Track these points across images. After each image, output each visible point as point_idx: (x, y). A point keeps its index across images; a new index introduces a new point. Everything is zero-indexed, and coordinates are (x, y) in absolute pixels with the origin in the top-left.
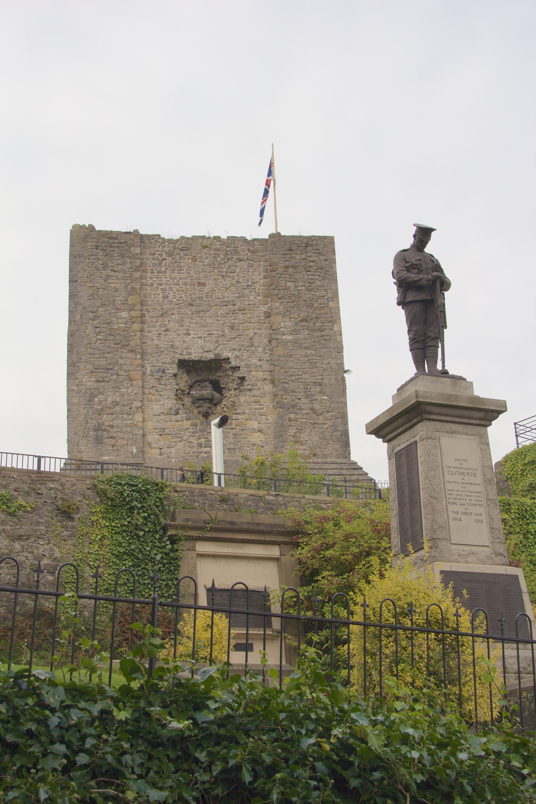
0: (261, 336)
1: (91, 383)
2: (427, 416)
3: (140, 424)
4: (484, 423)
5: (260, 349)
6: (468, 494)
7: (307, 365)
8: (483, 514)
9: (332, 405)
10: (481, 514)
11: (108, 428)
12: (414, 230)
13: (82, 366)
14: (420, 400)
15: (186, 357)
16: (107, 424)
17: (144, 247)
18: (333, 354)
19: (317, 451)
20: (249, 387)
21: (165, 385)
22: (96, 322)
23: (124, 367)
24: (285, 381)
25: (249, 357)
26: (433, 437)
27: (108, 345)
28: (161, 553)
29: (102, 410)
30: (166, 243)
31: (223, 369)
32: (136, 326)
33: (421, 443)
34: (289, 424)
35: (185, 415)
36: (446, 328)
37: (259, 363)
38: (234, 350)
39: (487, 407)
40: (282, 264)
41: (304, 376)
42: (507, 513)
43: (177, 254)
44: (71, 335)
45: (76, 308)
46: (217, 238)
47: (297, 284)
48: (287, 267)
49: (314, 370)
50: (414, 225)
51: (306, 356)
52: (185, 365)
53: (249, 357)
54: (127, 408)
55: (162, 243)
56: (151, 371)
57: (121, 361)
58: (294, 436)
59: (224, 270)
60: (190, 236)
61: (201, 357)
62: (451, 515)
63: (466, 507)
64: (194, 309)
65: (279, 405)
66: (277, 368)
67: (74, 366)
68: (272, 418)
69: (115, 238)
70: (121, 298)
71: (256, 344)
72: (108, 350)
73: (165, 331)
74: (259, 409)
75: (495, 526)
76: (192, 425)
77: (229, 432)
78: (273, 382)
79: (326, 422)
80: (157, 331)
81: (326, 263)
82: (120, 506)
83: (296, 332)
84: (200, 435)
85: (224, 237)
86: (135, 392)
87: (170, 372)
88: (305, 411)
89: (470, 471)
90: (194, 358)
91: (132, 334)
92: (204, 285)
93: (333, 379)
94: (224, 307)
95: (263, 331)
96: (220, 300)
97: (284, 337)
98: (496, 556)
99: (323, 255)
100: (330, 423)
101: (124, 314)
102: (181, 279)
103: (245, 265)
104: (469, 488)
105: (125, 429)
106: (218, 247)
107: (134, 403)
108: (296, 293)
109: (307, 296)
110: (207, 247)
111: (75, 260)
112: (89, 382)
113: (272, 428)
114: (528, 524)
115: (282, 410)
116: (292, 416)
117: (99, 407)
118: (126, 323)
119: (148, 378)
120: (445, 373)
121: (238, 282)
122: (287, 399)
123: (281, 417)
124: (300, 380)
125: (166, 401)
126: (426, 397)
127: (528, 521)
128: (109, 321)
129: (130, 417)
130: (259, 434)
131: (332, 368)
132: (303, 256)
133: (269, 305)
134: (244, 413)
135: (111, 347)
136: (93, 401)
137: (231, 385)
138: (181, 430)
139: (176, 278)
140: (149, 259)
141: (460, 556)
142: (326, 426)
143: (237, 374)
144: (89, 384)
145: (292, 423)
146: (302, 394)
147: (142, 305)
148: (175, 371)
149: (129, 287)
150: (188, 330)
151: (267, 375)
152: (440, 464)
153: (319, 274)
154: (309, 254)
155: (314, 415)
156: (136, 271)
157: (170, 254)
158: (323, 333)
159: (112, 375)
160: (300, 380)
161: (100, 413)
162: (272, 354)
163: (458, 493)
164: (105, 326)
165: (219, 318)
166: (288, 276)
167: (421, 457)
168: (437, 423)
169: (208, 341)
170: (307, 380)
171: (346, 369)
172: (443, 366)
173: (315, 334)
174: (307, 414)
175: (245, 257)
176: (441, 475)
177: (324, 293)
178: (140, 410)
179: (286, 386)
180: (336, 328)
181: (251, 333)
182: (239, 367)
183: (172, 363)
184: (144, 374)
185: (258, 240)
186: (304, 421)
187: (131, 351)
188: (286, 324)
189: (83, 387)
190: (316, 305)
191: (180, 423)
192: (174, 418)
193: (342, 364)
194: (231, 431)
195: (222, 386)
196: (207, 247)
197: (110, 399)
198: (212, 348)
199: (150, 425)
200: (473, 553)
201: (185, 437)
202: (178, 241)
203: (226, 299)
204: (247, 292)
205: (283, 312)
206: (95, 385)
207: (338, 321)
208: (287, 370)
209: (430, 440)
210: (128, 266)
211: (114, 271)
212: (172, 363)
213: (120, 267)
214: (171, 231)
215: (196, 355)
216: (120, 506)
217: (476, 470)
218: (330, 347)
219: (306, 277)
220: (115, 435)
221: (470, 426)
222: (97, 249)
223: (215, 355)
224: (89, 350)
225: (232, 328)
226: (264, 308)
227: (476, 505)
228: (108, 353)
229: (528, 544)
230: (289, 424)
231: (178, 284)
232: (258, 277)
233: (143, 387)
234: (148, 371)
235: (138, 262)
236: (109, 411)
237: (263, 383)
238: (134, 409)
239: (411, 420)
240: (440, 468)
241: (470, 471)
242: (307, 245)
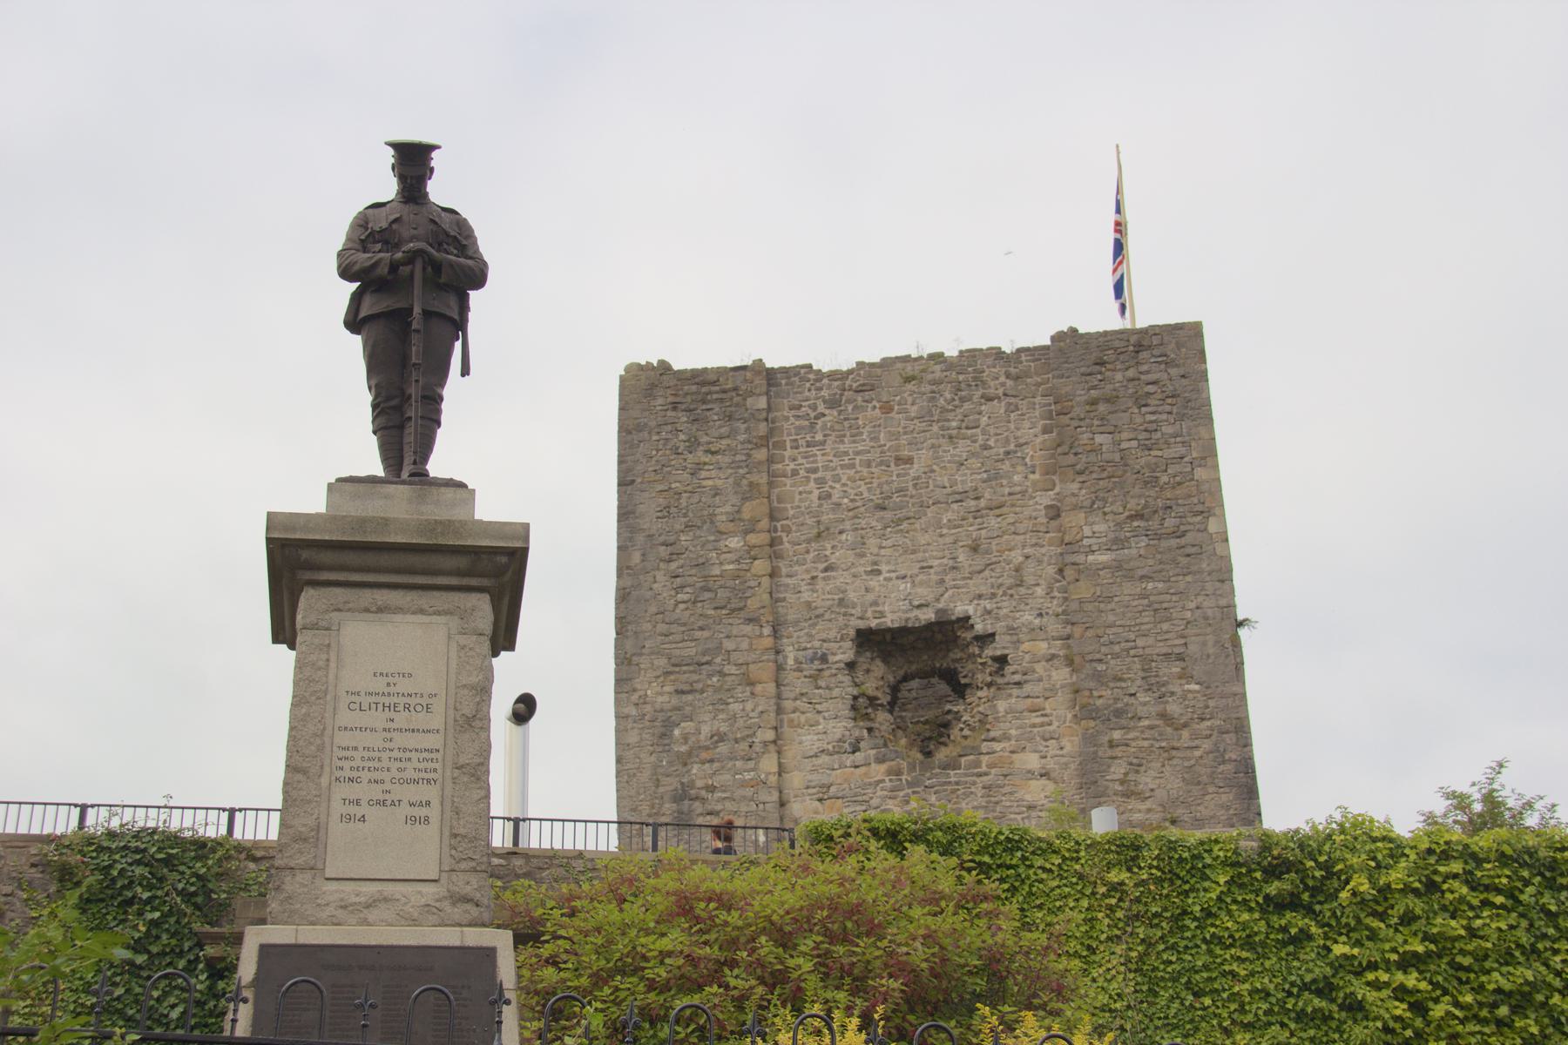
0: (1040, 562)
1: (666, 698)
2: (308, 575)
3: (773, 779)
5: (1039, 591)
6: (401, 755)
7: (1147, 617)
8: (436, 803)
9: (1211, 703)
10: (428, 803)
11: (703, 793)
12: (389, 156)
13: (644, 662)
15: (873, 624)
16: (699, 783)
17: (777, 395)
18: (1209, 586)
19: (1180, 811)
20: (1017, 678)
21: (828, 688)
22: (673, 566)
23: (734, 656)
24: (1098, 656)
25: (1015, 610)
27: (699, 611)
28: (184, 1001)
29: (690, 754)
30: (825, 381)
31: (960, 642)
32: (761, 566)
34: (1110, 753)
35: (873, 752)
37: (1037, 621)
38: (980, 597)
39: (469, 543)
40: (1081, 396)
41: (1140, 642)
42: (1129, 870)
43: (849, 401)
44: (623, 597)
45: (631, 539)
46: (937, 357)
47: (1117, 437)
48: (1094, 402)
49: (1165, 626)
51: (1143, 596)
52: (871, 641)
53: (1015, 610)
54: (744, 746)
55: (817, 380)
56: (796, 660)
57: (729, 645)
58: (1122, 782)
59: (954, 424)
60: (877, 360)
61: (907, 620)
62: (337, 808)
63: (387, 786)
64: (888, 515)
65: (1086, 713)
66: (1078, 631)
67: (630, 664)
68: (1070, 745)
69: (714, 383)
70: (728, 508)
71: (1030, 580)
72: (700, 623)
73: (826, 570)
74: (1042, 725)
75: (462, 831)
76: (889, 773)
77: (974, 783)
78: (1070, 662)
79: (1197, 742)
80: (807, 571)
82: (102, 900)
83: (1119, 543)
84: (907, 795)
85: (951, 352)
86: (760, 708)
87: (838, 658)
88: (1146, 723)
89: (412, 701)
90: (890, 624)
91: (752, 583)
92: (910, 461)
93: (1210, 643)
94: (955, 506)
95: (1043, 550)
96: (949, 490)
97: (1091, 558)
98: (454, 904)
99: (1177, 366)
100: (1207, 745)
101: (734, 543)
102: (858, 453)
103: (1000, 408)
104: (400, 740)
105: (739, 793)
106: (938, 375)
107: (759, 733)
108: (1117, 457)
109: (1143, 461)
110: (913, 378)
111: (629, 438)
112: (659, 695)
113: (1072, 766)
114: (1186, 893)
115: (1092, 723)
116: (1117, 735)
117: (684, 748)
118: (738, 561)
119: (790, 677)
121: (986, 447)
122: (1104, 697)
123: (1089, 739)
124: (1132, 652)
125: (832, 723)
127: (1187, 887)
128: (701, 561)
129: (751, 764)
130: (1044, 781)
131: (1206, 618)
133: (1057, 489)
134: (1006, 737)
135: (706, 616)
136: (671, 736)
138: (865, 786)
139: (846, 453)
140: (787, 419)
141: (344, 907)
142: (1197, 753)
143: (989, 652)
144: (660, 699)
145: (1118, 752)
146: (1139, 682)
147: (772, 518)
148: (849, 655)
149: (745, 482)
150: (875, 563)
151: (1057, 647)
153: (1168, 408)
154: (1145, 368)
155: (1169, 730)
156: (758, 446)
157: (833, 403)
158: (1183, 541)
159: (710, 676)
160: (1132, 652)
161: (685, 760)
162: (1066, 599)
163: (366, 754)
164: (693, 572)
165: (945, 531)
166: (1096, 422)
168: (338, 591)
169: (921, 584)
170: (1148, 651)
171: (1240, 617)
173: (1164, 544)
174: (1151, 727)
175: (1000, 391)
177: (1182, 450)
178: (772, 747)
179: (1100, 667)
180: (1213, 526)
181: (1017, 557)
182: (993, 635)
183: (842, 639)
184: (780, 668)
185: (1027, 350)
187: (750, 620)
188: (1096, 528)
189: (648, 708)
190: (1165, 479)
191: (862, 770)
192: (849, 759)
193: (1232, 606)
194: (978, 780)
195: (963, 681)
196: (913, 378)
197: (706, 730)
198: (930, 598)
199: (795, 780)
200: (386, 900)
201: (874, 802)
202: (850, 372)
203: (959, 488)
204: (1006, 466)
206: (675, 701)
207: (1217, 511)
208: (1100, 632)
210: (742, 437)
211: (713, 453)
212: (842, 639)
213: (724, 442)
214: (835, 349)
215: (895, 617)
216: (102, 900)
217: (431, 696)
218: (1200, 572)
219: (1139, 420)
220: (719, 807)
221: (436, 594)
222: (675, 409)
223: (938, 612)
224: (661, 627)
225: (975, 549)
226: (1045, 499)
227: (416, 782)
228: (701, 629)
229: (1183, 943)
230: (1110, 753)
231: (852, 466)
232: (1031, 431)
233: (779, 696)
234: (791, 662)
235: (763, 428)
236: (704, 755)
237: (1048, 666)
238: (758, 748)
241: (412, 701)
242: (1139, 348)
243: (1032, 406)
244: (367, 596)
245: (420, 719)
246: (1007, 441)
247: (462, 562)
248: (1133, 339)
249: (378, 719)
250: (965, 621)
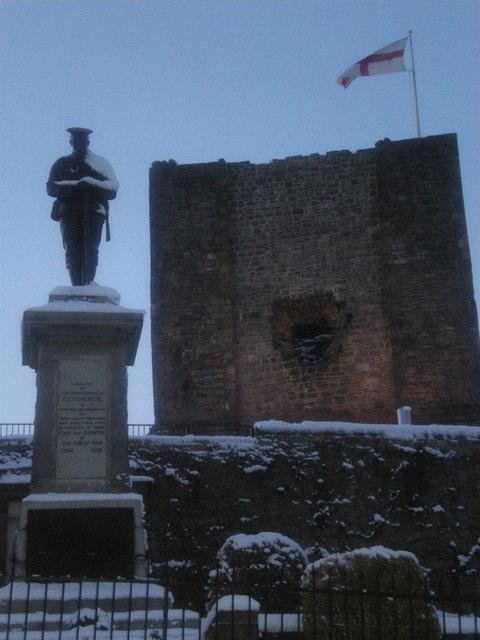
12: (68, 137)
50: (69, 130)
52: (280, 305)
68: (385, 357)
95: (372, 258)
97: (396, 261)
140: (236, 191)
226: (370, 231)
227: (95, 433)
250: (330, 295)
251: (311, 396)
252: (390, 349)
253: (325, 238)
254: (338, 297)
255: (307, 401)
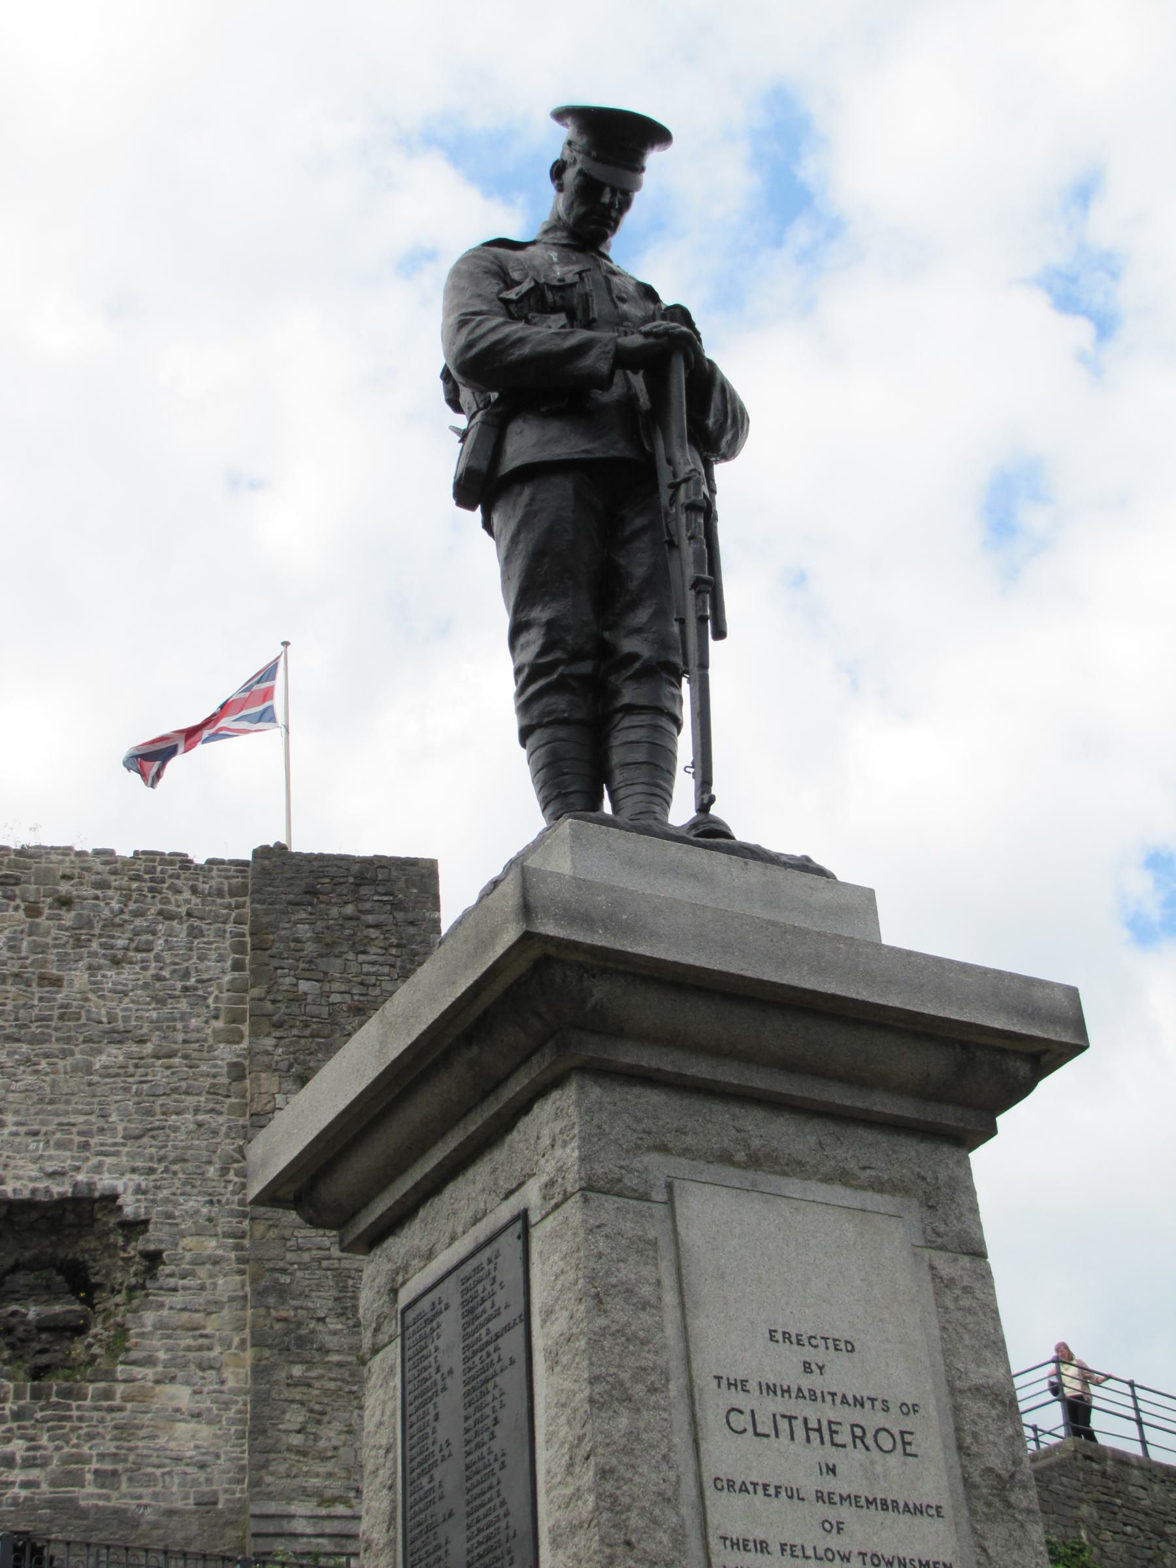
2: (592, 1049)
4: (949, 1116)
14: (549, 928)
20: (172, 1281)
24: (281, 1264)
26: (631, 1181)
31: (98, 1226)
33: (550, 1223)
36: (720, 634)
46: (105, 855)
47: (326, 987)
50: (561, 115)
59: (120, 943)
74: (200, 1348)
81: (412, 930)
84: (10, 1430)
88: (335, 1358)
90: (10, 1195)
92: (57, 982)
95: (221, 1119)
99: (404, 909)
108: (325, 1011)
116: (297, 1371)
120: (709, 832)
123: (260, 1371)
124: (325, 1264)
126: (586, 920)
132: (349, 909)
133: (245, 1044)
134: (149, 1361)
137: (118, 1275)
143: (140, 1244)
152: (676, 1365)
153: (392, 960)
154: (368, 906)
160: (325, 1264)
165: (96, 1078)
167: (548, 1313)
168: (655, 1098)
172: (705, 803)
174: (340, 1365)
175: (183, 910)
176: (681, 1439)
182: (146, 1222)
186: (332, 1385)
194: (108, 1417)
195: (95, 1279)
203: (120, 1025)
205: (283, 1065)
208: (287, 1233)
209: (611, 1203)
219: (354, 968)
221: (869, 1136)
226: (226, 1054)
239: (499, 1083)
240: (675, 1388)
241: (872, 1419)
243: (221, 934)
244: (722, 1124)
245: (892, 1475)
246: (186, 975)
247: (911, 1061)
248: (356, 868)
249: (796, 1462)
250: (111, 1199)
251: (29, 1463)
252: (249, 1355)
253: (110, 1056)
254: (130, 1206)
255: (17, 1475)
